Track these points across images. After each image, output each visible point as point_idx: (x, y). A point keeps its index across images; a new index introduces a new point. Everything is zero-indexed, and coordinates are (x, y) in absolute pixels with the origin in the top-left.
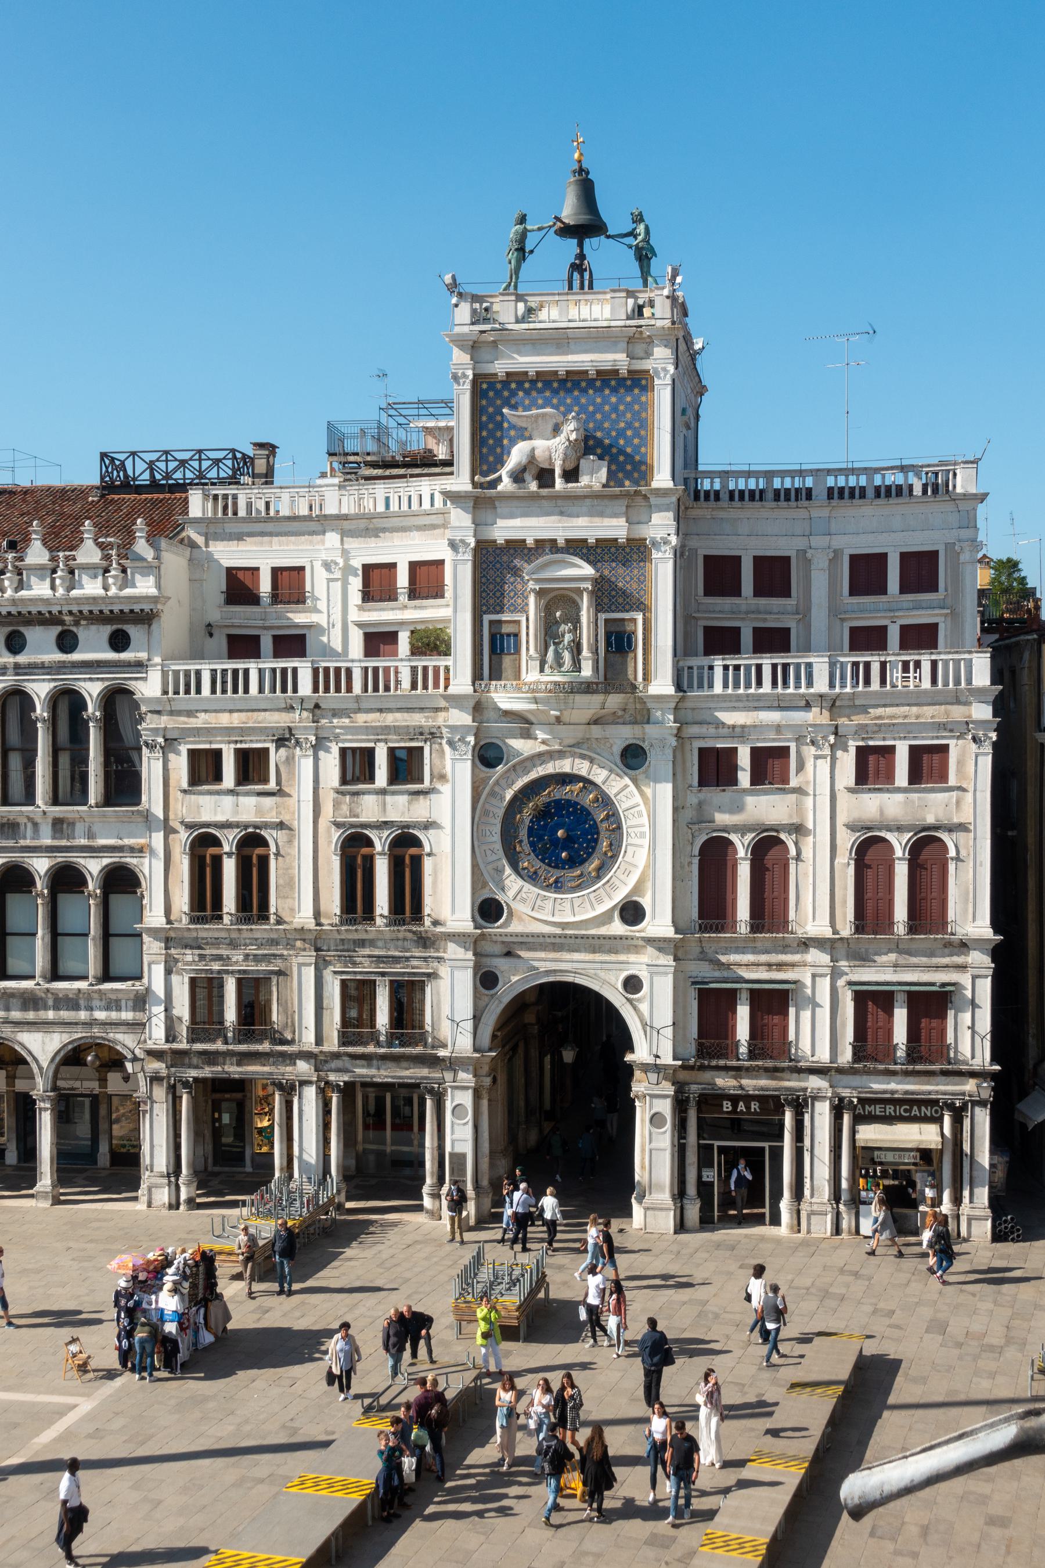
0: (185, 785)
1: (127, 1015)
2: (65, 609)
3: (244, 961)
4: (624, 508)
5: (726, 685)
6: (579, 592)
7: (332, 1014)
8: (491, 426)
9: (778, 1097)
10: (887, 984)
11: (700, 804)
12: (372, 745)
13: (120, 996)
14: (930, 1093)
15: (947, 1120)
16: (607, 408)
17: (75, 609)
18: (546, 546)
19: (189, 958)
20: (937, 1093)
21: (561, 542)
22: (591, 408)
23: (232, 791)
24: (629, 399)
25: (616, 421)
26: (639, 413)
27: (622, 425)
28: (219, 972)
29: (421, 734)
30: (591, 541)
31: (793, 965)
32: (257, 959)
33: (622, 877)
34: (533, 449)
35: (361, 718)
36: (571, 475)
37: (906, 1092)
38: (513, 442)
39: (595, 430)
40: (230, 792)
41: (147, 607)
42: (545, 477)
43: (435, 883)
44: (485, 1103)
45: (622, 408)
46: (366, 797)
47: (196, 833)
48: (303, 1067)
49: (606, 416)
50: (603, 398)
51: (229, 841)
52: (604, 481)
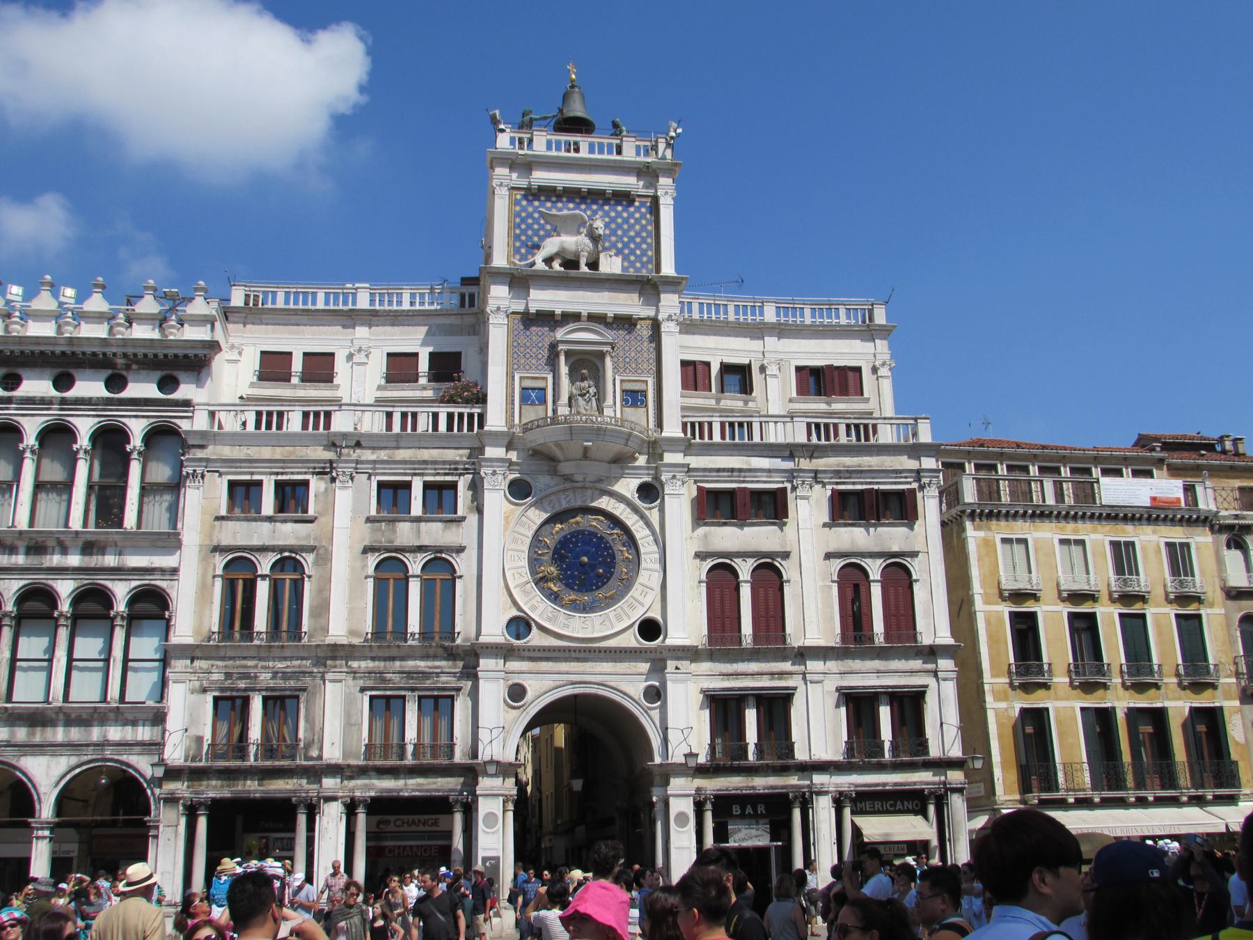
0: (223, 512)
1: (144, 733)
2: (119, 351)
3: (272, 678)
5: (723, 437)
6: (601, 356)
7: (360, 730)
8: (523, 226)
9: (786, 795)
10: (873, 687)
11: (706, 536)
12: (408, 478)
13: (140, 716)
14: (915, 783)
15: (931, 809)
16: (619, 220)
17: (130, 351)
18: (571, 318)
19: (215, 677)
20: (921, 783)
21: (584, 313)
23: (270, 519)
24: (637, 215)
25: (628, 230)
27: (632, 234)
28: (246, 690)
29: (456, 469)
30: (611, 315)
31: (791, 673)
32: (286, 676)
33: (640, 598)
34: (562, 242)
35: (402, 454)
36: (594, 265)
37: (896, 784)
38: (542, 239)
39: (610, 235)
40: (270, 519)
41: (200, 352)
43: (465, 603)
44: (510, 815)
45: (632, 221)
46: (401, 524)
47: (230, 557)
48: (329, 783)
49: (619, 226)
50: (617, 212)
51: (265, 564)
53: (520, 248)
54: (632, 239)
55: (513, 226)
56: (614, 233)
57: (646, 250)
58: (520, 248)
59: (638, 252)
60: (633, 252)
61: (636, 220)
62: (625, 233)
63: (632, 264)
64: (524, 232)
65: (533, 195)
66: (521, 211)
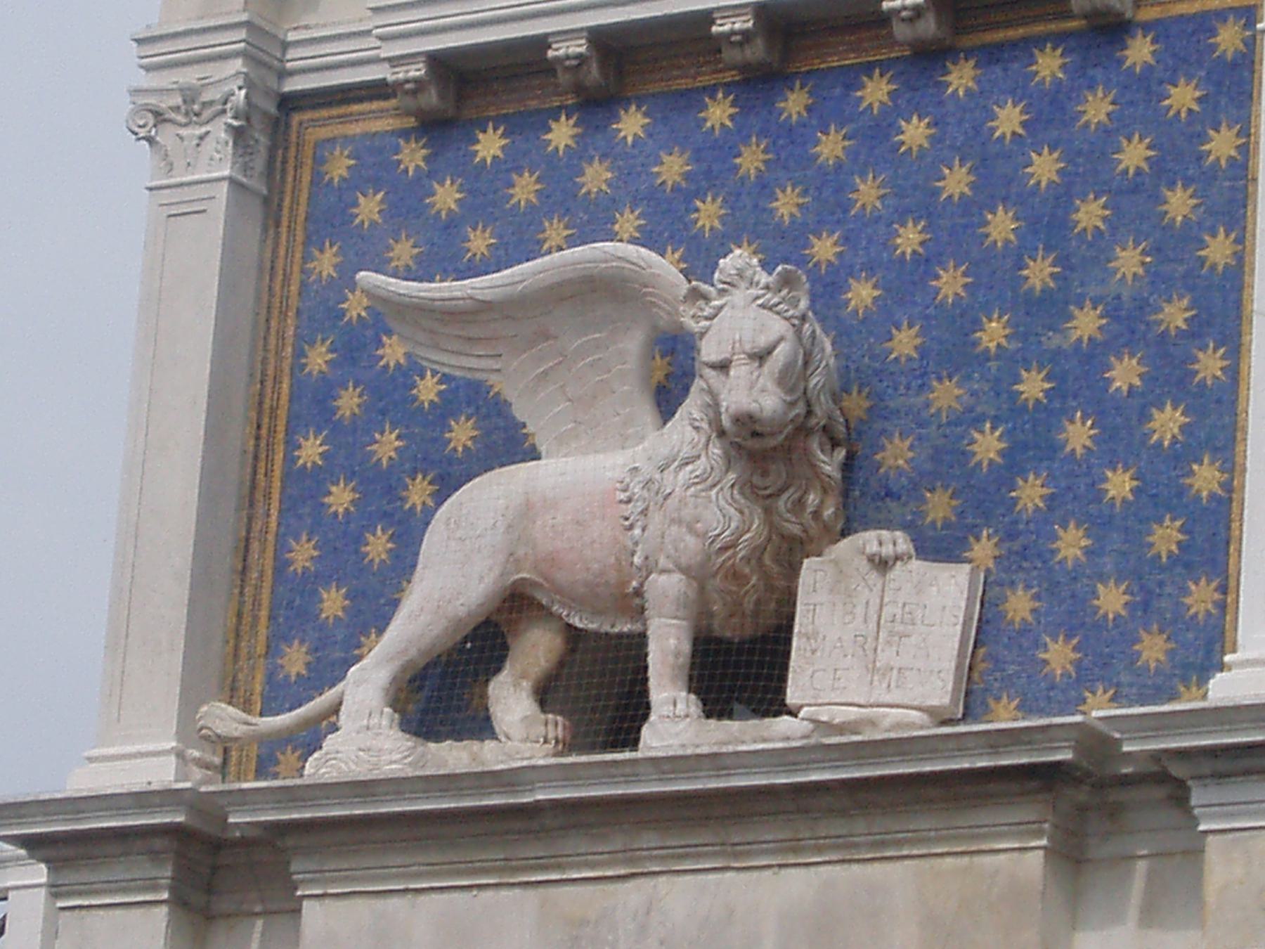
4: (1034, 862)
8: (349, 402)
26: (1191, 235)
27: (1086, 323)
34: (528, 509)
39: (921, 373)
42: (600, 690)
45: (1090, 214)
54: (1079, 378)
60: (1076, 495)
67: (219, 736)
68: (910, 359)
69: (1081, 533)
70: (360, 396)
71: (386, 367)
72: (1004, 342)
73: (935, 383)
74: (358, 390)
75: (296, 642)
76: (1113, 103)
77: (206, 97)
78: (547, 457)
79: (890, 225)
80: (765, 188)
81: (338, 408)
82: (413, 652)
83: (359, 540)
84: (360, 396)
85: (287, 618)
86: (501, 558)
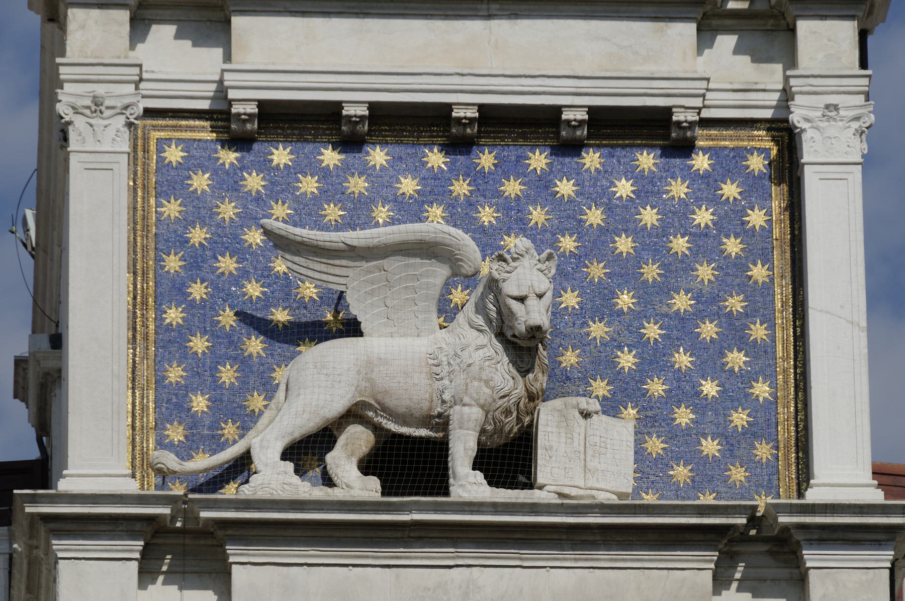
8: (198, 291)
16: (624, 244)
22: (568, 243)
24: (703, 217)
26: (740, 265)
27: (682, 302)
34: (369, 364)
39: (583, 315)
49: (625, 272)
52: (627, 484)
53: (185, 390)
54: (681, 329)
55: (151, 290)
56: (599, 303)
57: (748, 378)
58: (185, 390)
59: (710, 388)
60: (684, 390)
61: (699, 236)
62: (652, 297)
63: (683, 444)
64: (201, 317)
65: (240, 141)
66: (187, 222)
67: (168, 469)
68: (574, 308)
69: (688, 411)
70: (206, 288)
71: (223, 273)
72: (631, 305)
73: (591, 323)
74: (205, 284)
75: (176, 423)
76: (688, 187)
77: (108, 103)
78: (370, 335)
79: (554, 234)
80: (471, 204)
81: (191, 293)
82: (297, 434)
83: (214, 370)
84: (206, 288)
85: (167, 408)
86: (353, 388)
